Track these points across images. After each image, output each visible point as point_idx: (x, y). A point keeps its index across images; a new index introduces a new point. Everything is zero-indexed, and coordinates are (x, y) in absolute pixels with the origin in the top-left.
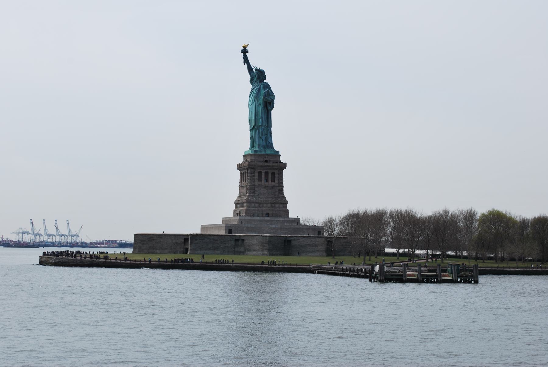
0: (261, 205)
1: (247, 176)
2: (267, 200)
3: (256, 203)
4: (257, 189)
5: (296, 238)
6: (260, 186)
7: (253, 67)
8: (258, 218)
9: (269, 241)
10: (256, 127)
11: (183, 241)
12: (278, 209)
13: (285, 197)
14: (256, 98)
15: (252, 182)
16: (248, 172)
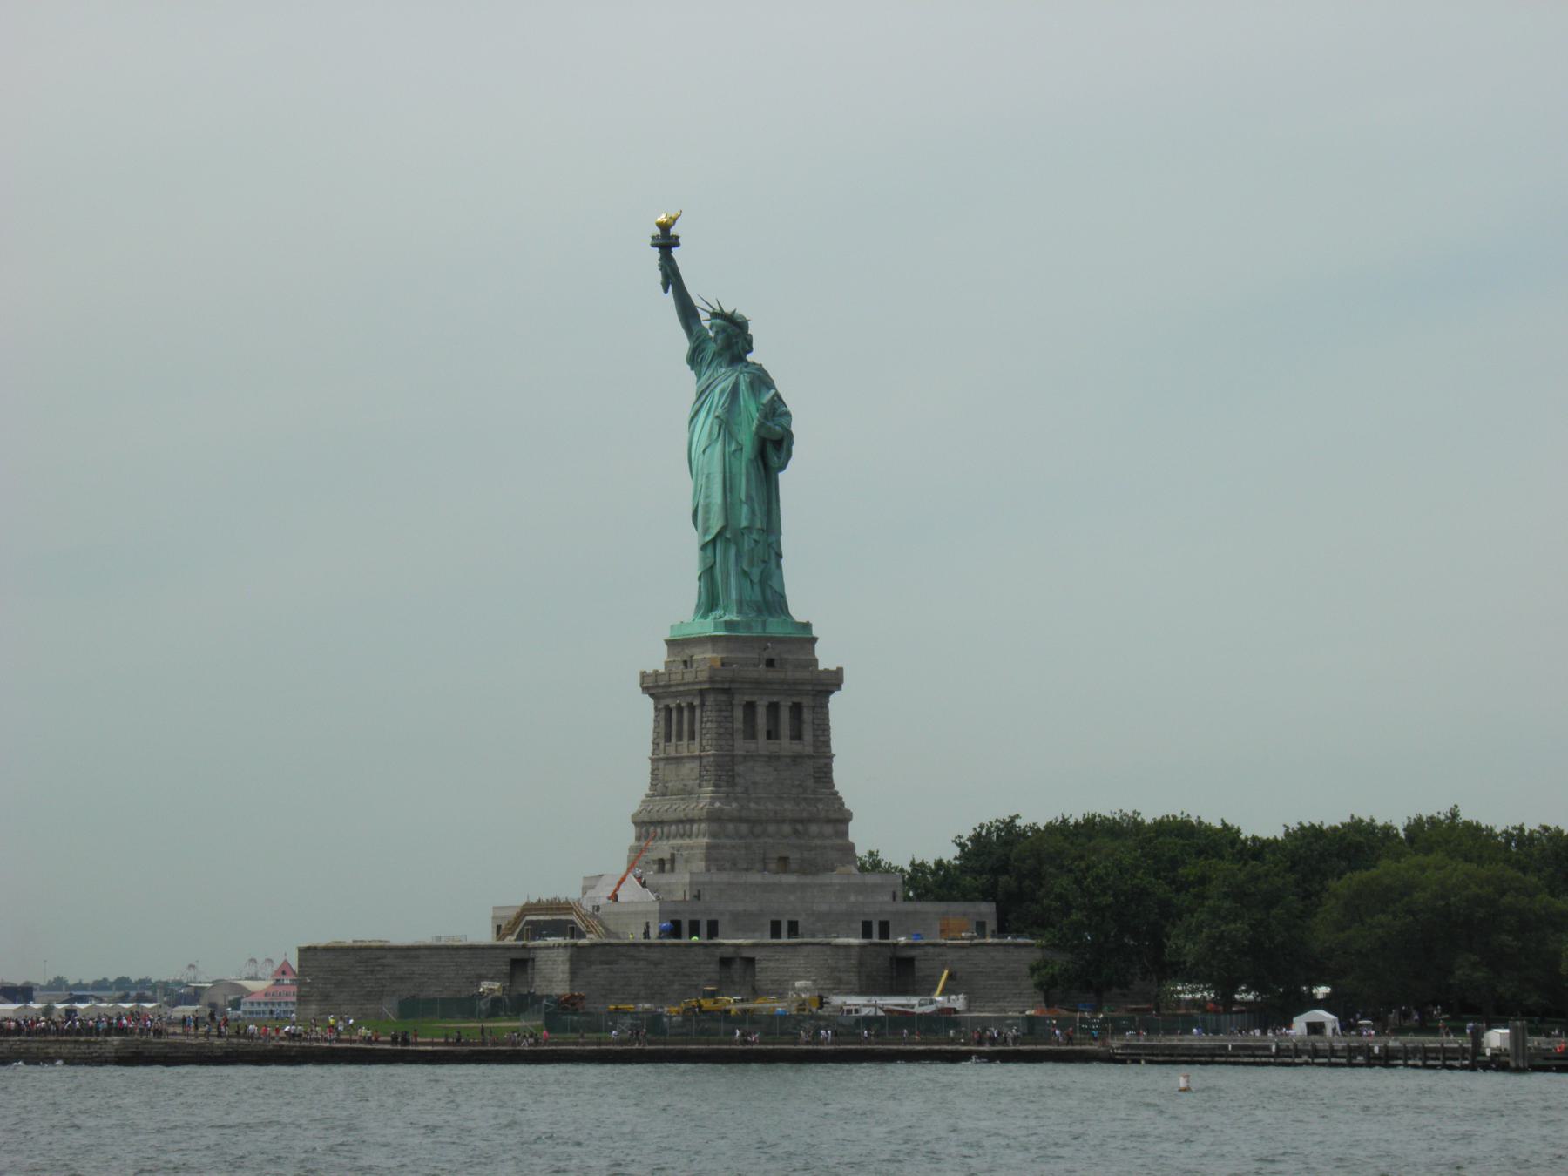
0: (758, 829)
1: (702, 717)
2: (777, 808)
3: (741, 820)
4: (740, 769)
5: (931, 950)
6: (752, 756)
7: (697, 302)
8: (756, 878)
9: (861, 964)
10: (728, 536)
11: (506, 968)
12: (818, 842)
13: (840, 795)
14: (726, 425)
15: (723, 742)
16: (702, 705)
